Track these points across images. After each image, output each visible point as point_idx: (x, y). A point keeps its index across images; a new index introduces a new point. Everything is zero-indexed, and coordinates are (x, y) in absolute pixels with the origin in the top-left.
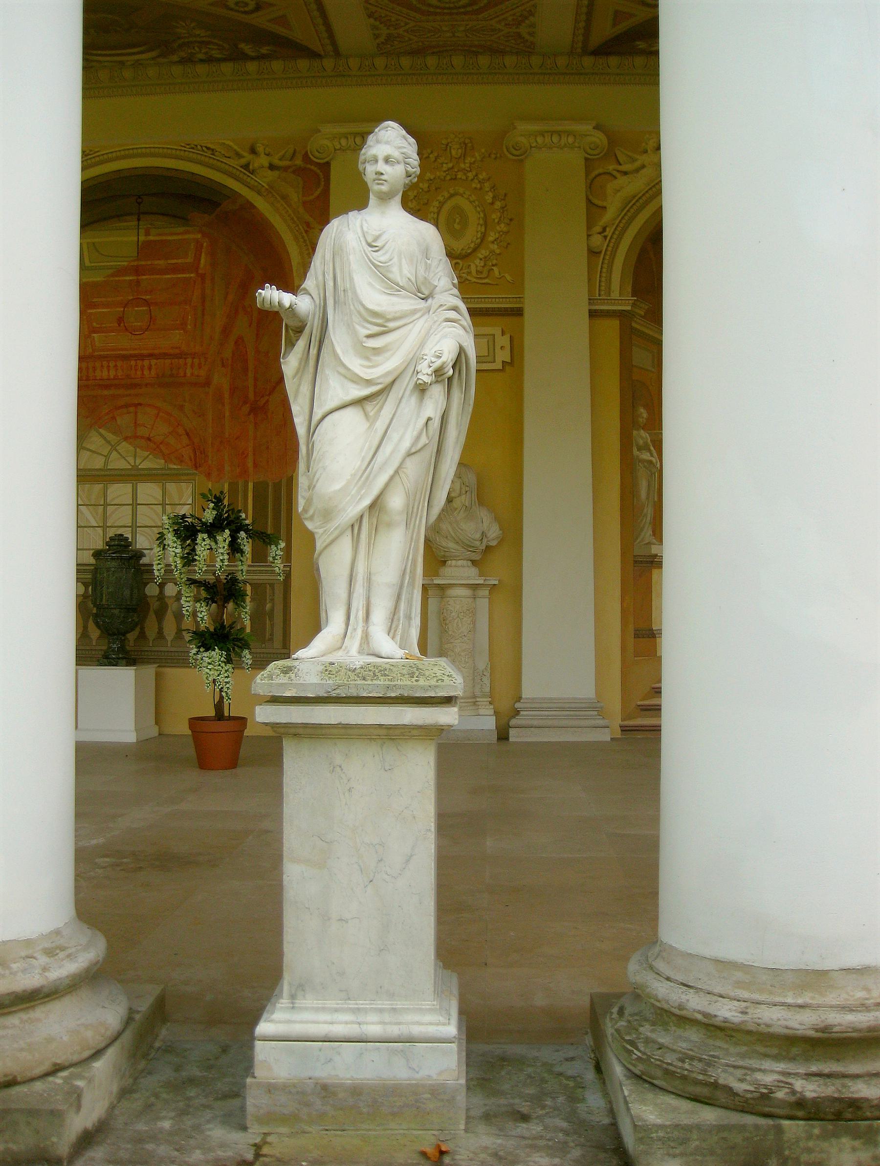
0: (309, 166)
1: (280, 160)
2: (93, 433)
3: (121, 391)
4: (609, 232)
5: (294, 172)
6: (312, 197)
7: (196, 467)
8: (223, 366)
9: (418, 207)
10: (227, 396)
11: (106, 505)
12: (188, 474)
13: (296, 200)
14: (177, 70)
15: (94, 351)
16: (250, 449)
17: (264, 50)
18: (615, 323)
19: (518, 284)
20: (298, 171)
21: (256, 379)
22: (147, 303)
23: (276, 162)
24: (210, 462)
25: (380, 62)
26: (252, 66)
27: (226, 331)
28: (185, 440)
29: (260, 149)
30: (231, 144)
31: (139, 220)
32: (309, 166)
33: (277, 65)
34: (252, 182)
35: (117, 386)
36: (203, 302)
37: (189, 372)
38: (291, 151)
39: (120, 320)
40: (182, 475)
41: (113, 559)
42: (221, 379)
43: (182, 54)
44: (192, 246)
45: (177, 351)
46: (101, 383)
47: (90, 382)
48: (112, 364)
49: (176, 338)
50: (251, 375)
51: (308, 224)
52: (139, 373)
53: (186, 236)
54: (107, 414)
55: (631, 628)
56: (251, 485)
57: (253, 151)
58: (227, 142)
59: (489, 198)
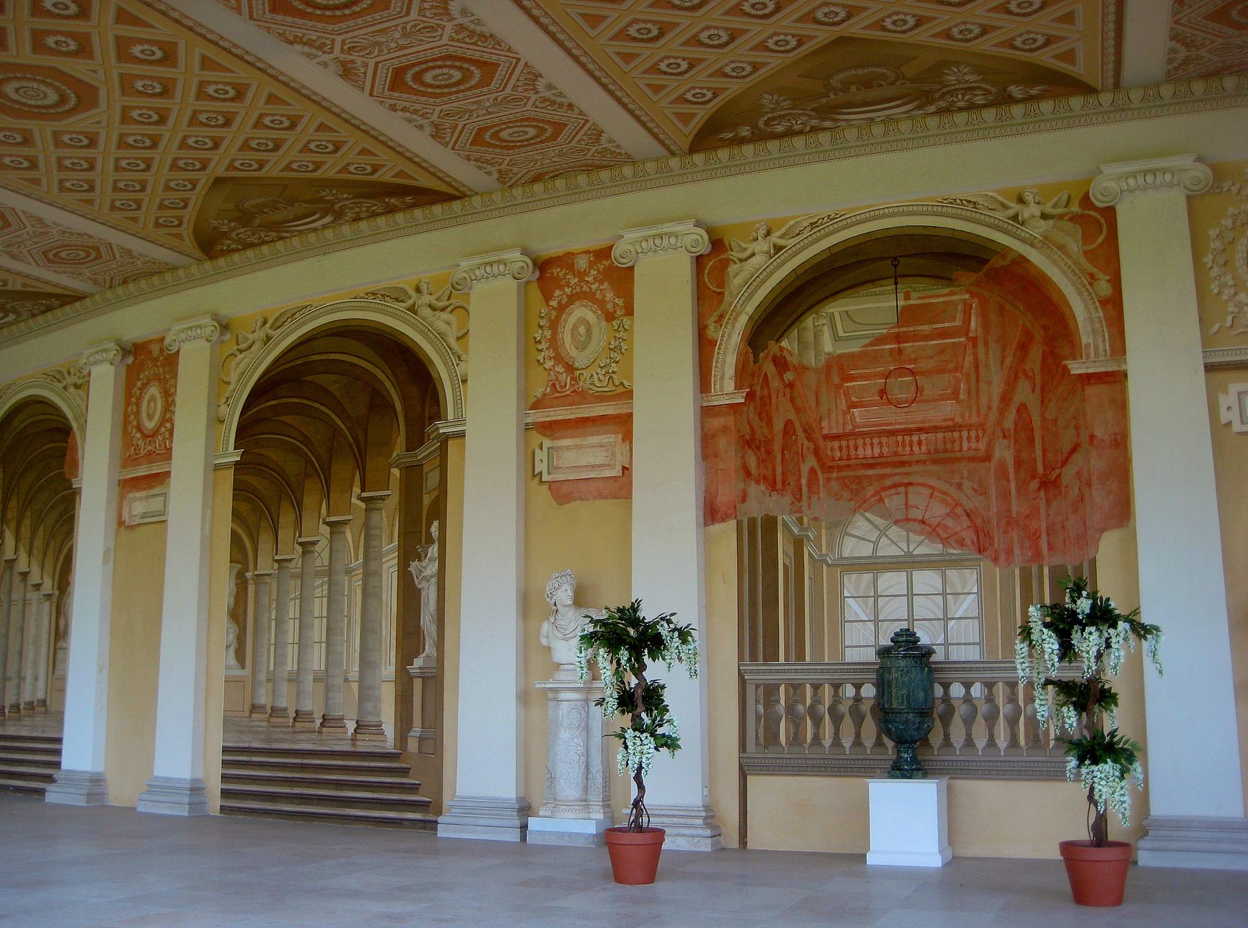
0: (1087, 212)
1: (1054, 207)
2: (858, 517)
3: (888, 471)
5: (1071, 219)
6: (1094, 246)
7: (980, 552)
8: (1004, 437)
9: (1221, 248)
10: (1011, 470)
11: (877, 597)
12: (970, 560)
13: (1076, 249)
14: (933, 122)
15: (854, 427)
16: (1044, 529)
17: (1034, 92)
20: (1074, 219)
21: (1044, 451)
22: (912, 373)
23: (1048, 209)
24: (996, 545)
25: (1167, 91)
26: (1017, 110)
27: (1006, 399)
28: (965, 518)
29: (1029, 197)
30: (995, 195)
31: (896, 283)
32: (1087, 212)
33: (1046, 106)
34: (1023, 234)
35: (882, 465)
36: (977, 367)
37: (965, 446)
38: (1065, 197)
39: (882, 393)
40: (965, 560)
41: (905, 657)
42: (1004, 452)
43: (942, 104)
44: (960, 307)
45: (950, 423)
46: (864, 462)
47: (852, 462)
48: (876, 441)
49: (947, 410)
50: (1038, 445)
51: (1092, 276)
52: (908, 449)
53: (953, 298)
54: (873, 496)
56: (1046, 570)
57: (1021, 200)
58: (990, 194)
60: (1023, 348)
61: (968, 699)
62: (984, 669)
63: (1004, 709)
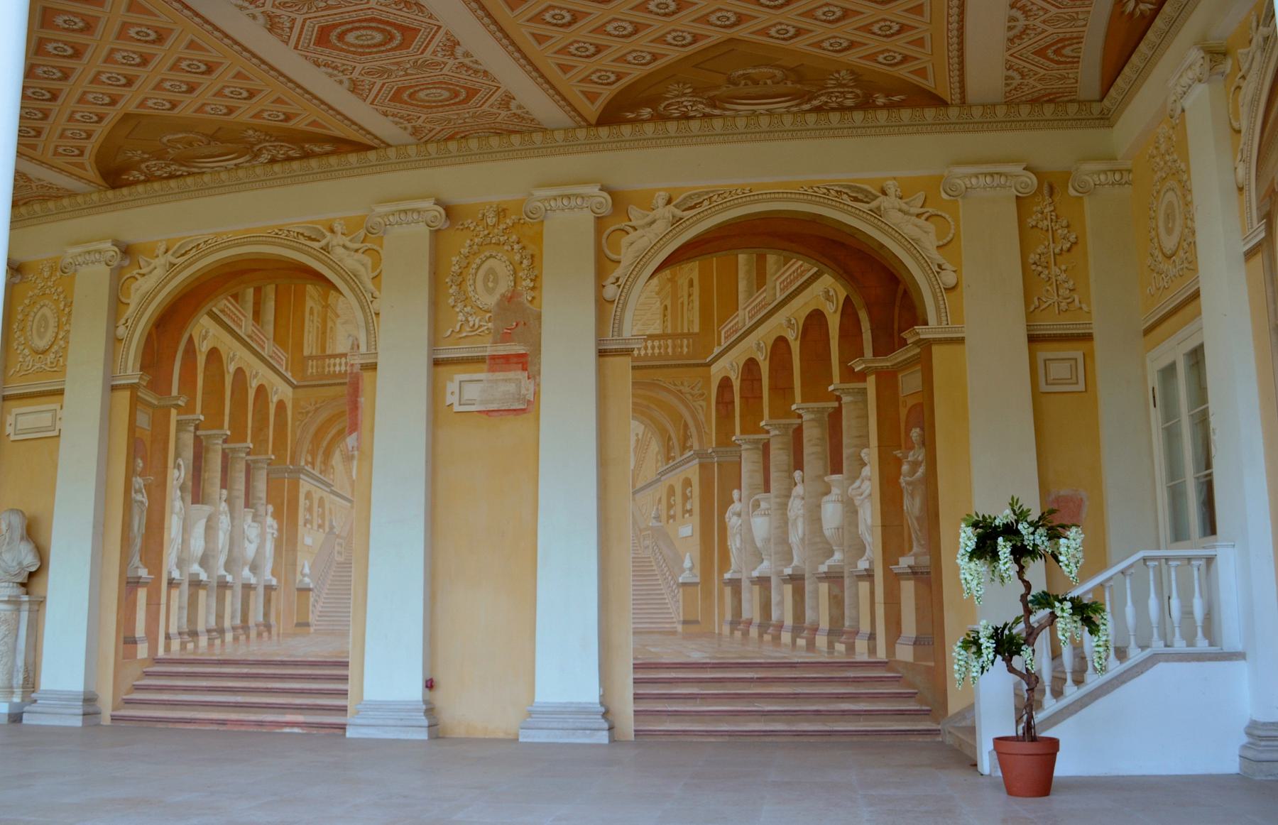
4: (129, 323)
18: (127, 394)
19: (59, 369)
55: (122, 635)
59: (62, 306)
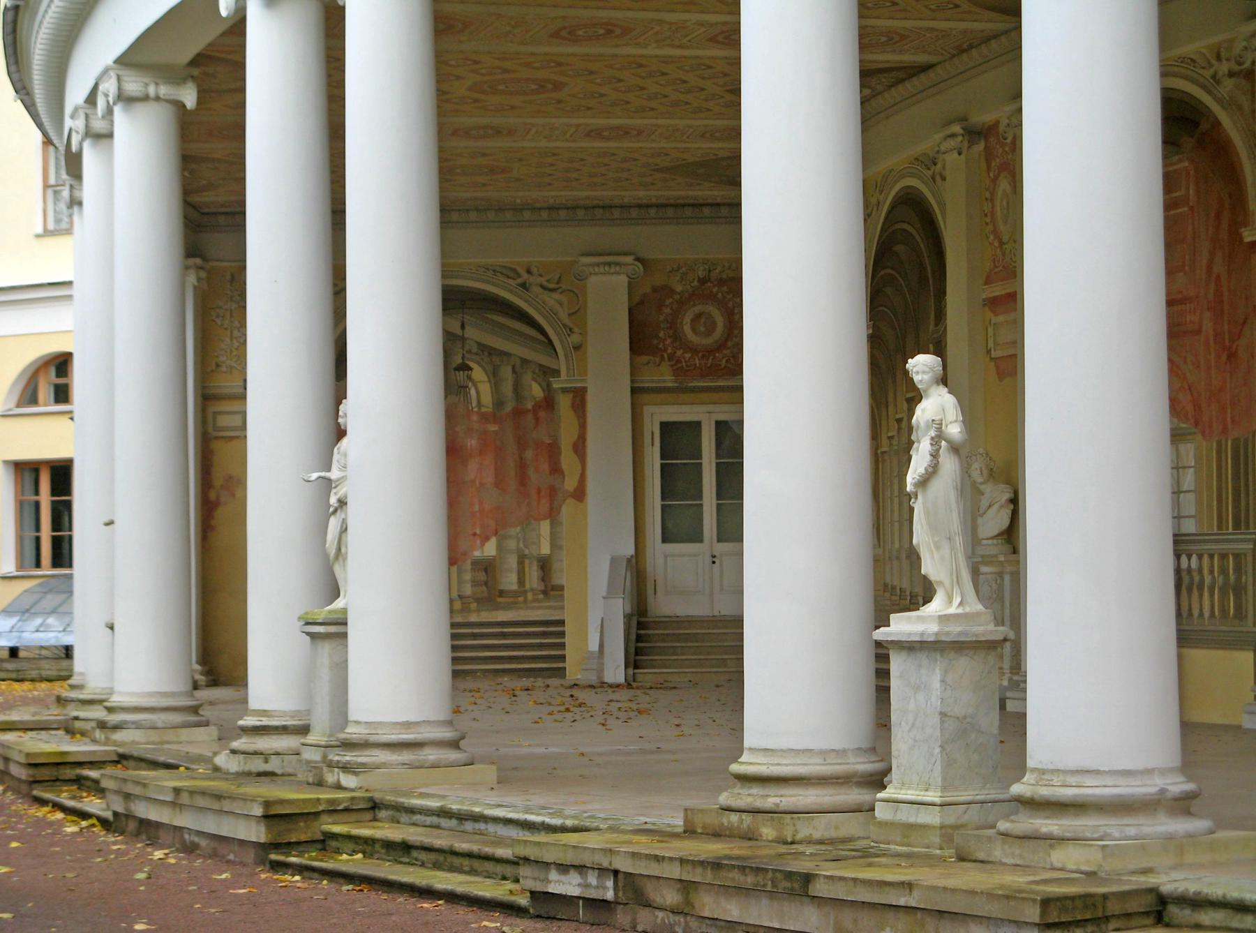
27: (1209, 269)
56: (1229, 443)
57: (1219, 58)
60: (1218, 216)
61: (1189, 570)
62: (1199, 541)
63: (1208, 579)
